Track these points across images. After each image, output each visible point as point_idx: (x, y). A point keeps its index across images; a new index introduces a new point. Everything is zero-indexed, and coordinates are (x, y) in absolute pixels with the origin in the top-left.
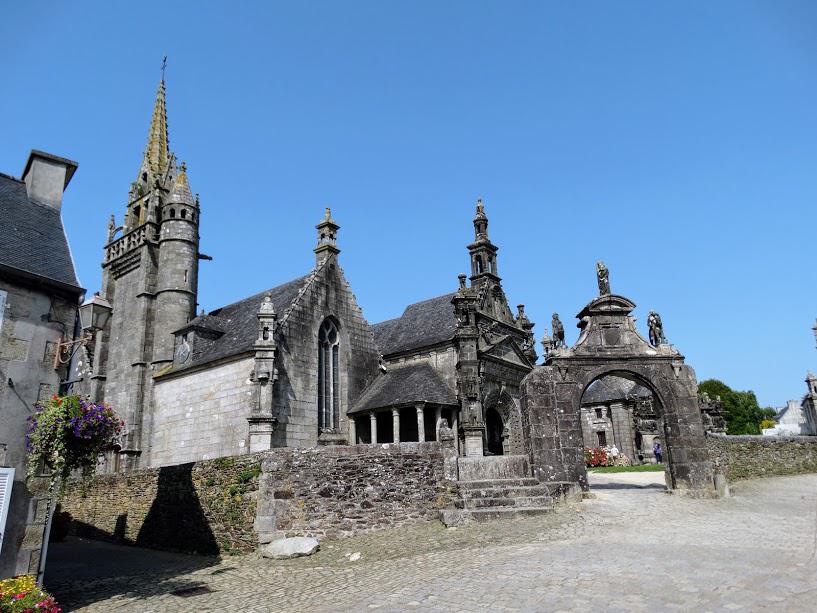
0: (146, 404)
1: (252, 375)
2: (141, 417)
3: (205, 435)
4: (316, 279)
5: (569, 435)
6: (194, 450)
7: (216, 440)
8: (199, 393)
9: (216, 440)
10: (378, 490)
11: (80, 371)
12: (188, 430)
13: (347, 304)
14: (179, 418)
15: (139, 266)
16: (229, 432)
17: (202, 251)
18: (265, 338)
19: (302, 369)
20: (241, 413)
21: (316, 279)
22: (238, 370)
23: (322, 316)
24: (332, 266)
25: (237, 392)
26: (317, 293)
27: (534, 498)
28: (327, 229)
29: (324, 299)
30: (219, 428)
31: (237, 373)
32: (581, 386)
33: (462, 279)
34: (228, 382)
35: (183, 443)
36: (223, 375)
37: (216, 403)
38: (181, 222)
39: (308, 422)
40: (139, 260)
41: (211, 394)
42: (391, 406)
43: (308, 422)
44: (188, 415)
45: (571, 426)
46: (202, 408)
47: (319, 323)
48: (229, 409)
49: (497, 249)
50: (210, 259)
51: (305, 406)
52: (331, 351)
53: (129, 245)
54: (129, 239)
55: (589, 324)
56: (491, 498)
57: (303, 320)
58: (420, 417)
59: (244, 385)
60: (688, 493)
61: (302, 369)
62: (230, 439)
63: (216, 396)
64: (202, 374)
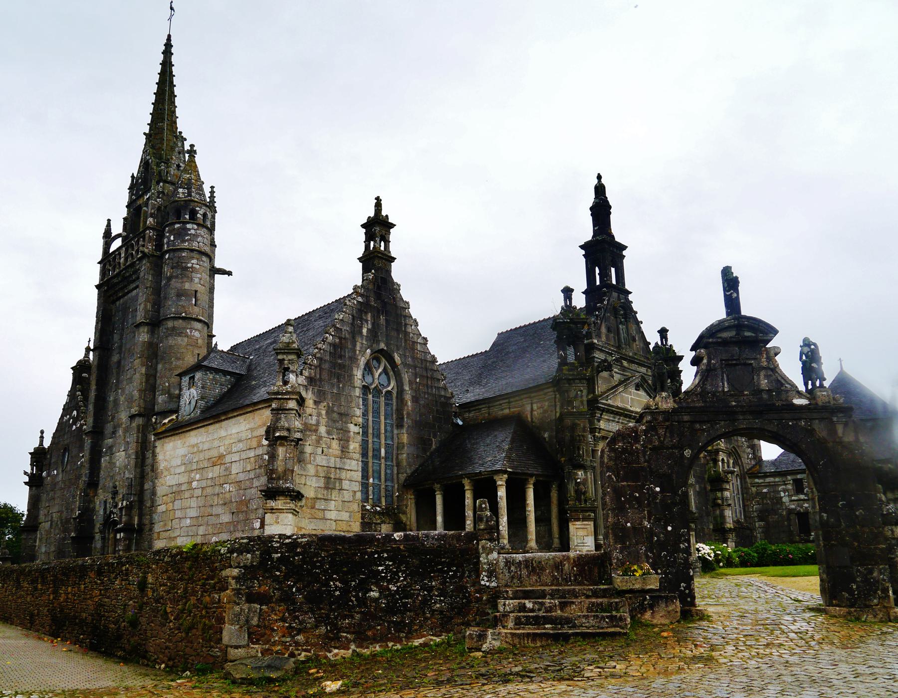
0: (148, 469)
1: (268, 432)
2: (142, 485)
3: (215, 511)
4: (360, 299)
6: (201, 530)
7: (226, 518)
8: (208, 455)
9: (226, 518)
10: (386, 597)
11: (74, 423)
12: (193, 503)
13: (406, 334)
14: (184, 488)
15: (137, 287)
16: (241, 509)
17: (218, 264)
18: (286, 383)
19: (339, 425)
20: (256, 483)
21: (360, 299)
22: (252, 425)
23: (368, 351)
25: (252, 454)
26: (361, 319)
27: (600, 615)
29: (370, 326)
30: (231, 502)
31: (252, 430)
32: (687, 453)
33: (568, 292)
34: (240, 441)
35: (188, 521)
36: (234, 431)
37: (226, 469)
38: (189, 226)
40: (138, 278)
41: (221, 456)
42: (462, 477)
43: (347, 496)
44: (195, 484)
46: (210, 476)
47: (362, 361)
48: (242, 477)
49: (625, 248)
50: (229, 273)
51: (343, 475)
53: (126, 259)
54: (127, 250)
55: (705, 361)
56: (541, 614)
57: (341, 357)
58: (502, 493)
59: (260, 445)
60: (849, 613)
61: (339, 425)
62: (241, 517)
63: (228, 459)
64: (211, 428)
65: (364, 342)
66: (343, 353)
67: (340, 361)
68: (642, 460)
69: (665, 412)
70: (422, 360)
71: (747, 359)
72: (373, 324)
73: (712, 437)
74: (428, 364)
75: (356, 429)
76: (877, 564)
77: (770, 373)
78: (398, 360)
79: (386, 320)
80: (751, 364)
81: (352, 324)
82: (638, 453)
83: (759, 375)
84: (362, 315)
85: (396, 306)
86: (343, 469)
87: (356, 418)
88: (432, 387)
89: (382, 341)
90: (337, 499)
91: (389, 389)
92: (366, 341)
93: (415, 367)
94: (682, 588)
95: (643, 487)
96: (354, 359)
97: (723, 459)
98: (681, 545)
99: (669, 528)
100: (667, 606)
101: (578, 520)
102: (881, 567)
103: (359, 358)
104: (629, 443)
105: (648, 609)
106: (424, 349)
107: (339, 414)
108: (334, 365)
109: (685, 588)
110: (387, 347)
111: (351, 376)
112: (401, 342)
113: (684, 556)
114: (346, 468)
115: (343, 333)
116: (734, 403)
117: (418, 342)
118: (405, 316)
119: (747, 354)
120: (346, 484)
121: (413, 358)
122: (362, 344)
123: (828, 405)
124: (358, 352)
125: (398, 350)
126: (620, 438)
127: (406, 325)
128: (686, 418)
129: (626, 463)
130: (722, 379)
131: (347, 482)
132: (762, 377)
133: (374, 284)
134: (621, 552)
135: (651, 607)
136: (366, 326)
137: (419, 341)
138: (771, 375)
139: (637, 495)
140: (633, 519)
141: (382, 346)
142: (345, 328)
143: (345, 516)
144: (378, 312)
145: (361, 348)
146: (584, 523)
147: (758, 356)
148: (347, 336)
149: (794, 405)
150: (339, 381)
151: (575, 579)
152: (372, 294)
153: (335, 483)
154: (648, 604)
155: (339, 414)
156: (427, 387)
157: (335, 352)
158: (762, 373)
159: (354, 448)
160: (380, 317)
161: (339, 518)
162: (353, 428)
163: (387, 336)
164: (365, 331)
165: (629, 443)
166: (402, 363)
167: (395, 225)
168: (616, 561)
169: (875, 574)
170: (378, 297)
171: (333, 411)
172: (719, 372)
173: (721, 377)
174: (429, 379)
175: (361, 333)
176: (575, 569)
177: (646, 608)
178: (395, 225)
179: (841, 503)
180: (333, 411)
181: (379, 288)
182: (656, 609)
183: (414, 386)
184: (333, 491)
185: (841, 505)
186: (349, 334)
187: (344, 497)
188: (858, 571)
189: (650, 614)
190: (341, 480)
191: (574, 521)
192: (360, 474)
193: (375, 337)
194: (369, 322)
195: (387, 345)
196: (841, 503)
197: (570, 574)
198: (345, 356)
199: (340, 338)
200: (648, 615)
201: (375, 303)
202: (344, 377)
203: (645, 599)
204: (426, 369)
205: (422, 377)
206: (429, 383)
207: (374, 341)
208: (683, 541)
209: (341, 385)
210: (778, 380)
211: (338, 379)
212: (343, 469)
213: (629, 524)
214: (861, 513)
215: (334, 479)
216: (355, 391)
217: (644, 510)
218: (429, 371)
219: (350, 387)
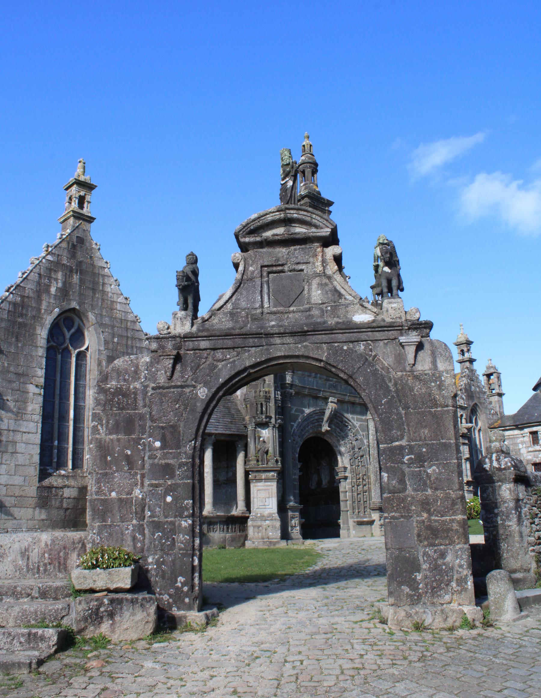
4: (49, 257)
5: (166, 494)
13: (103, 292)
19: (15, 385)
21: (49, 257)
23: (57, 310)
24: (81, 241)
28: (74, 188)
29: (60, 285)
39: (21, 459)
43: (21, 459)
45: (172, 476)
47: (49, 320)
51: (18, 437)
52: (74, 359)
57: (22, 315)
65: (52, 301)
66: (24, 312)
67: (20, 320)
68: (140, 403)
69: (174, 337)
70: (121, 320)
71: (298, 263)
72: (64, 283)
73: (236, 371)
74: (129, 324)
75: (37, 391)
76: (452, 543)
77: (325, 280)
78: (92, 319)
79: (81, 280)
80: (302, 270)
81: (39, 283)
82: (135, 394)
83: (310, 285)
84: (50, 274)
85: (93, 265)
86: (18, 431)
87: (37, 379)
88: (132, 347)
89: (75, 300)
90: (8, 462)
91: (83, 349)
92: (55, 299)
93: (113, 327)
94: (179, 584)
95: (137, 441)
96: (38, 317)
97: (462, 416)
98: (183, 522)
99: (169, 499)
100: (133, 614)
101: (260, 480)
102: (458, 547)
103: (45, 317)
104: (125, 380)
105: (104, 619)
106: (125, 309)
107: (15, 374)
108: (14, 323)
109: (184, 584)
110: (80, 306)
111: (33, 336)
112: (97, 301)
113: (185, 539)
114: (21, 430)
115: (27, 292)
116: (273, 323)
117: (117, 302)
118: (104, 276)
119: (297, 258)
120: (20, 447)
121: (111, 318)
122: (49, 303)
123: (398, 320)
124: (43, 311)
125: (93, 309)
126: (115, 374)
127: (104, 284)
128: (204, 344)
129: (119, 409)
130: (261, 291)
131: (23, 445)
132: (314, 286)
133: (68, 243)
134: (99, 534)
135: (111, 615)
136: (55, 285)
137: (119, 300)
138: (326, 284)
139: (129, 452)
140: (119, 486)
141: (74, 304)
142: (29, 286)
143: (18, 480)
144: (71, 271)
145: (48, 306)
146: (266, 483)
147: (311, 260)
148: (31, 294)
149: (350, 322)
150: (18, 340)
151: (45, 570)
152: (65, 254)
153: (6, 446)
154: (106, 611)
155: (15, 374)
156: (127, 347)
157: (15, 309)
158: (315, 283)
159: (32, 410)
160: (72, 277)
161: (10, 483)
162: (32, 389)
163: (80, 294)
164: (53, 290)
165: (125, 380)
166: (98, 323)
167: (96, 186)
168: (90, 545)
169: (449, 558)
170: (73, 256)
171: (9, 372)
172: (258, 282)
173: (260, 289)
174: (129, 339)
175: (48, 292)
176: (46, 555)
177: (102, 618)
178: (96, 186)
179: (407, 457)
180: (9, 372)
181: (74, 246)
182: (117, 618)
183: (111, 346)
184: (4, 454)
185: (408, 460)
186: (34, 292)
187: (18, 461)
188: (425, 554)
189: (108, 626)
190: (14, 443)
191: (256, 482)
192: (39, 436)
193: (66, 295)
194: (59, 281)
195: (80, 304)
196: (407, 457)
197: (39, 562)
198: (26, 315)
199: (23, 297)
200: (105, 628)
201: (68, 262)
202: (25, 336)
203: (101, 604)
204: (127, 329)
205: (120, 336)
206: (129, 342)
207: (64, 299)
208: (186, 517)
209: (20, 345)
210: (336, 290)
211: (17, 338)
212: (18, 431)
213: (114, 494)
214: (434, 470)
215: (6, 442)
216: (37, 351)
217: (136, 474)
218: (129, 331)
219: (31, 347)
